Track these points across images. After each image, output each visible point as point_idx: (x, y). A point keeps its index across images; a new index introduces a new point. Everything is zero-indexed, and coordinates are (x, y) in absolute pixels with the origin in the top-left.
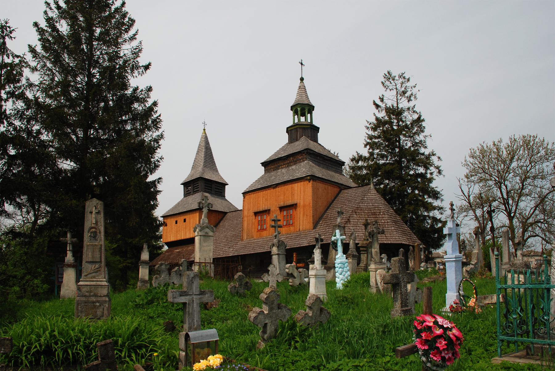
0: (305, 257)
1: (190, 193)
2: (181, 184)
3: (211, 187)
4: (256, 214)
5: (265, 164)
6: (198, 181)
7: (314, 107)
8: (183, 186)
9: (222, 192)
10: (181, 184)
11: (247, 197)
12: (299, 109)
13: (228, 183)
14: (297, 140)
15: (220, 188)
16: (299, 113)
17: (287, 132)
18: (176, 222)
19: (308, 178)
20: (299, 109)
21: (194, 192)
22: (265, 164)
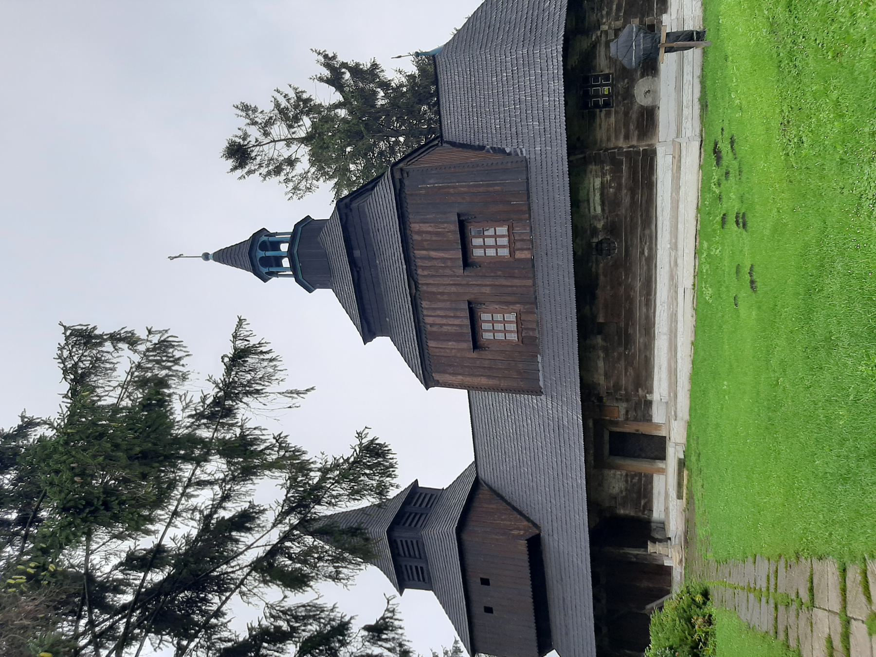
0: (598, 182)
1: (421, 568)
2: (401, 593)
3: (416, 514)
4: (476, 344)
5: (368, 335)
6: (395, 541)
7: (264, 229)
8: (407, 591)
9: (432, 495)
10: (401, 593)
11: (437, 376)
12: (261, 254)
13: (415, 479)
14: (325, 256)
15: (423, 496)
16: (270, 253)
17: (310, 291)
18: (489, 610)
19: (398, 176)
20: (261, 254)
21: (420, 558)
22: (368, 335)
